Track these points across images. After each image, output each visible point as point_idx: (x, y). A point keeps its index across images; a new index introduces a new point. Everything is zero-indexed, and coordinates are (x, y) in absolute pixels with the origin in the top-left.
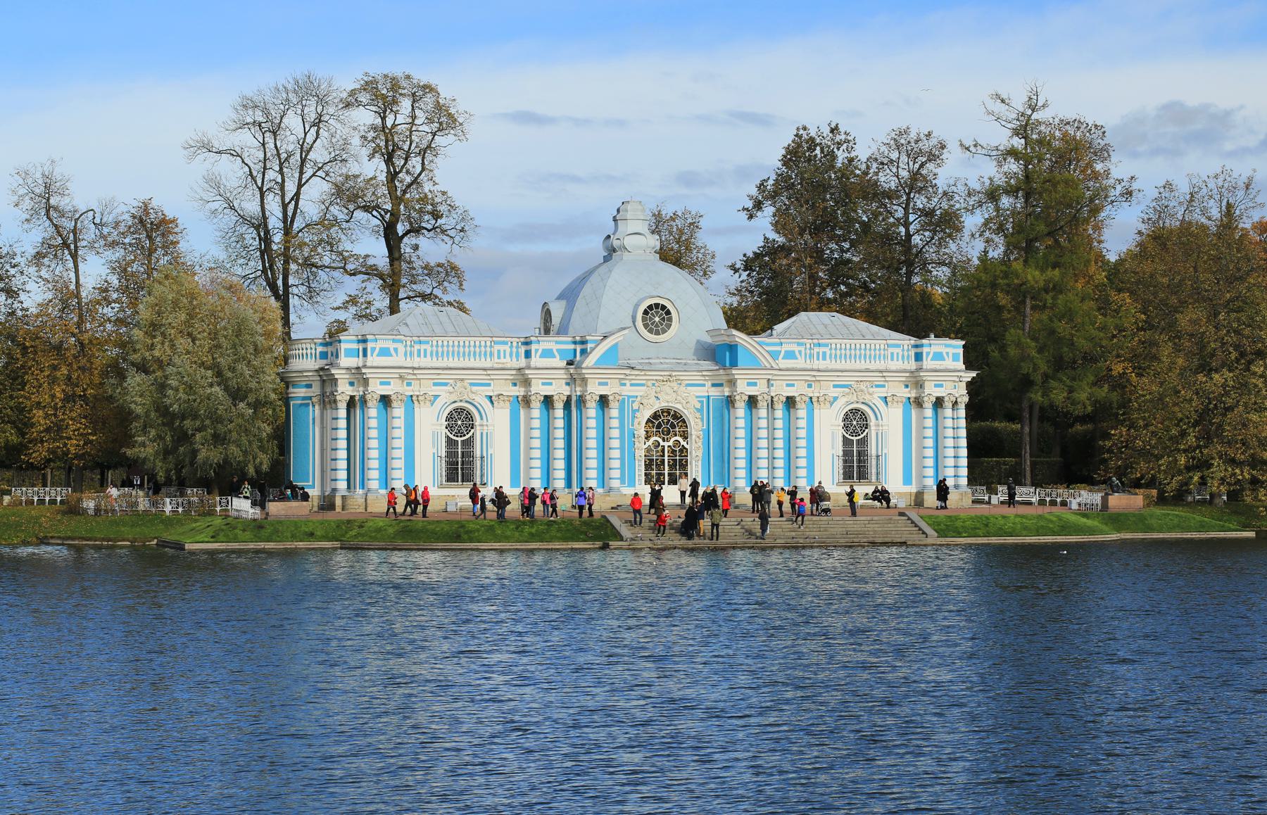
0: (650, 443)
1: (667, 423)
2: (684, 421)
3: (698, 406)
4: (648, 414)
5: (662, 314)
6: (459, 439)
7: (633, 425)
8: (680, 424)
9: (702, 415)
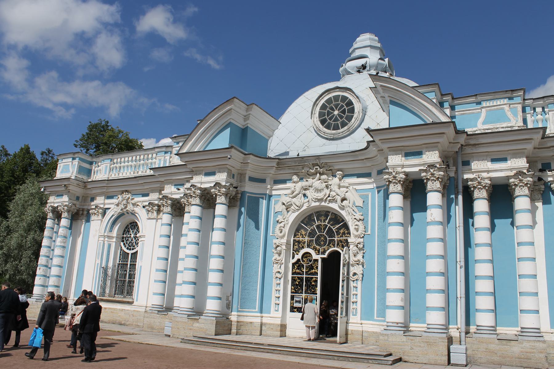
0: (299, 256)
1: (324, 229)
2: (346, 226)
3: (360, 203)
4: (292, 217)
5: (342, 106)
6: (130, 252)
7: (274, 232)
8: (342, 231)
9: (365, 214)
